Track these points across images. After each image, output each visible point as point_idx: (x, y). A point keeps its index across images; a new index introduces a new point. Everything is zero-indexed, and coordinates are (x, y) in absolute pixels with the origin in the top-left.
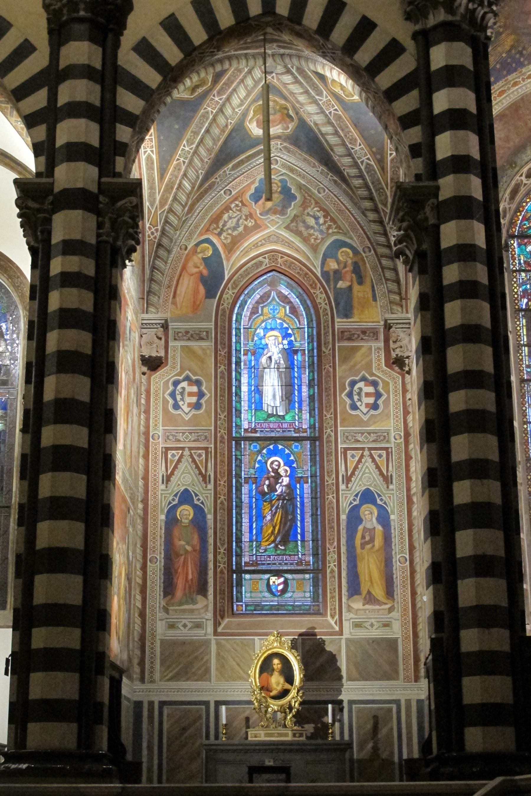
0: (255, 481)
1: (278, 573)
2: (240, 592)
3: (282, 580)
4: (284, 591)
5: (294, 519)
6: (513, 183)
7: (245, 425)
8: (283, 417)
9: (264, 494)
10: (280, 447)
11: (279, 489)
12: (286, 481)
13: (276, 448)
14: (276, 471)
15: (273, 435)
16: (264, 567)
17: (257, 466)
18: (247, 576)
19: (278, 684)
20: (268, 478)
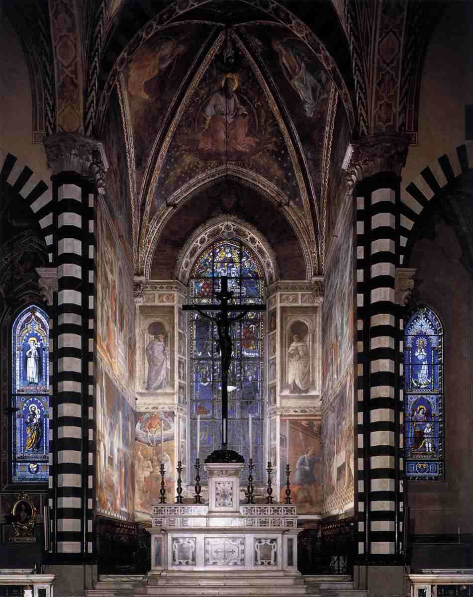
0: (24, 417)
1: (34, 462)
2: (15, 471)
3: (36, 466)
4: (37, 471)
5: (42, 436)
6: (192, 247)
7: (18, 388)
8: (37, 384)
9: (27, 423)
10: (36, 399)
11: (35, 421)
12: (38, 416)
13: (33, 399)
14: (33, 412)
15: (32, 393)
16: (27, 459)
17: (24, 409)
18: (19, 464)
19: (24, 516)
20: (29, 415)
